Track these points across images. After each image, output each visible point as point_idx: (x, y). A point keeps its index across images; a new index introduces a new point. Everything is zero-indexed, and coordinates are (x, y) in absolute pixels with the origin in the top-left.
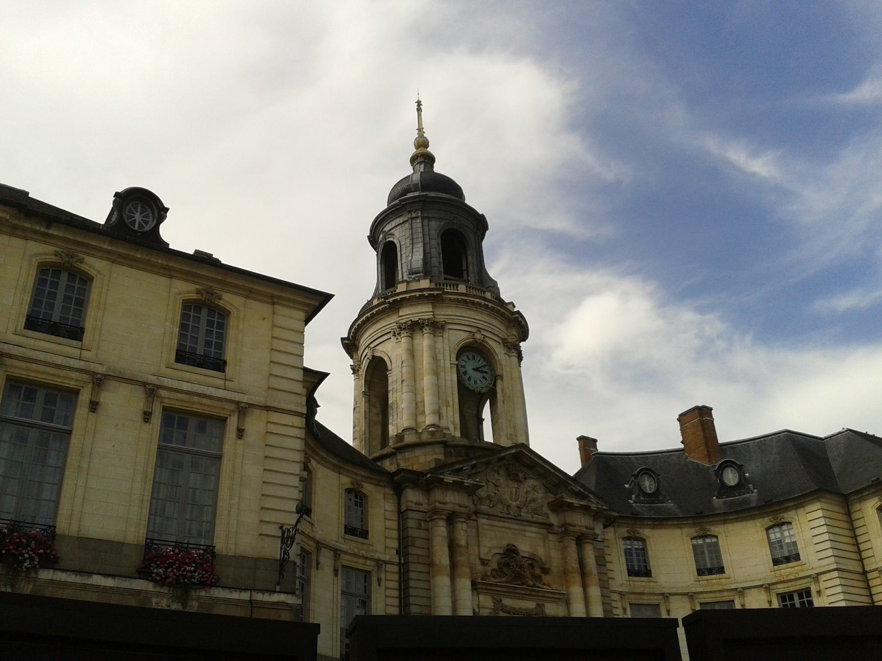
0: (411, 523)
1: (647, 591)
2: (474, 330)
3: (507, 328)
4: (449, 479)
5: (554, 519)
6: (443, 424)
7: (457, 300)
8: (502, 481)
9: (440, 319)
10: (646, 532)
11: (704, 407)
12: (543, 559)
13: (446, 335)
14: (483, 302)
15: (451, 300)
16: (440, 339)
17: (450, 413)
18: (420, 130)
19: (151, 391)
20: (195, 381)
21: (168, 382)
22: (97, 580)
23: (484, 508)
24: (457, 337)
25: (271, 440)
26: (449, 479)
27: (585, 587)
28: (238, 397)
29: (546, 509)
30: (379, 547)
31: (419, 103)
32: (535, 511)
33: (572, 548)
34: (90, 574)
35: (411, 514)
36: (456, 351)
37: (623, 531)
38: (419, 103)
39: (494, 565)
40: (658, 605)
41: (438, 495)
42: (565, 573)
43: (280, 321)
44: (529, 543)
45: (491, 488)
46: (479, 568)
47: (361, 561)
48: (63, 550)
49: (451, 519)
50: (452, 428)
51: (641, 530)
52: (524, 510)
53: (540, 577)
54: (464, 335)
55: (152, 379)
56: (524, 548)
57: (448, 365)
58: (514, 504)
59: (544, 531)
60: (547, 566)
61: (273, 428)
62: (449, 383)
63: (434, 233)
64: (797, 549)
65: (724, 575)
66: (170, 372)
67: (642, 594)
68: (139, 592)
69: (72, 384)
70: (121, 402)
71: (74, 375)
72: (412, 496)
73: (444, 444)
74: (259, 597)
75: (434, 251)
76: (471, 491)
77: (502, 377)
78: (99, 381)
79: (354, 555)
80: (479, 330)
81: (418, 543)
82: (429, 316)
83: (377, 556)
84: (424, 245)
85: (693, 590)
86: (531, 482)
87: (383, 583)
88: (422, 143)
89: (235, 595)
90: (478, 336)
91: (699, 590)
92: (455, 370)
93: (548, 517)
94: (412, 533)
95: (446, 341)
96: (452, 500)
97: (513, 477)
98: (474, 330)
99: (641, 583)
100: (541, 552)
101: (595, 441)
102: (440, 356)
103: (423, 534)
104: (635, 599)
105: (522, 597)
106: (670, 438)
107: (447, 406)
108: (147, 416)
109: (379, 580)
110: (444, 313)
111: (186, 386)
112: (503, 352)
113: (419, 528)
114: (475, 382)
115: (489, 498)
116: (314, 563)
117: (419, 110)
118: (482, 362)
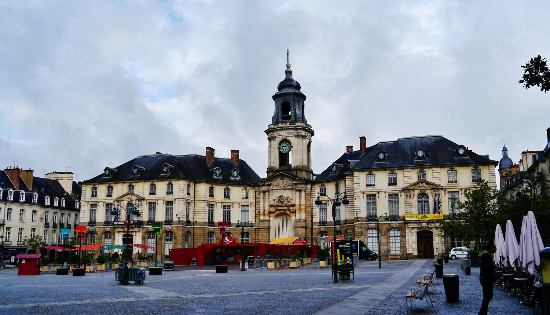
4: (261, 184)
10: (326, 184)
23: (274, 188)
26: (261, 184)
31: (288, 51)
33: (298, 193)
37: (320, 185)
38: (288, 51)
46: (273, 201)
49: (264, 192)
72: (257, 188)
73: (272, 171)
76: (270, 185)
88: (288, 66)
90: (284, 138)
96: (264, 188)
117: (288, 53)
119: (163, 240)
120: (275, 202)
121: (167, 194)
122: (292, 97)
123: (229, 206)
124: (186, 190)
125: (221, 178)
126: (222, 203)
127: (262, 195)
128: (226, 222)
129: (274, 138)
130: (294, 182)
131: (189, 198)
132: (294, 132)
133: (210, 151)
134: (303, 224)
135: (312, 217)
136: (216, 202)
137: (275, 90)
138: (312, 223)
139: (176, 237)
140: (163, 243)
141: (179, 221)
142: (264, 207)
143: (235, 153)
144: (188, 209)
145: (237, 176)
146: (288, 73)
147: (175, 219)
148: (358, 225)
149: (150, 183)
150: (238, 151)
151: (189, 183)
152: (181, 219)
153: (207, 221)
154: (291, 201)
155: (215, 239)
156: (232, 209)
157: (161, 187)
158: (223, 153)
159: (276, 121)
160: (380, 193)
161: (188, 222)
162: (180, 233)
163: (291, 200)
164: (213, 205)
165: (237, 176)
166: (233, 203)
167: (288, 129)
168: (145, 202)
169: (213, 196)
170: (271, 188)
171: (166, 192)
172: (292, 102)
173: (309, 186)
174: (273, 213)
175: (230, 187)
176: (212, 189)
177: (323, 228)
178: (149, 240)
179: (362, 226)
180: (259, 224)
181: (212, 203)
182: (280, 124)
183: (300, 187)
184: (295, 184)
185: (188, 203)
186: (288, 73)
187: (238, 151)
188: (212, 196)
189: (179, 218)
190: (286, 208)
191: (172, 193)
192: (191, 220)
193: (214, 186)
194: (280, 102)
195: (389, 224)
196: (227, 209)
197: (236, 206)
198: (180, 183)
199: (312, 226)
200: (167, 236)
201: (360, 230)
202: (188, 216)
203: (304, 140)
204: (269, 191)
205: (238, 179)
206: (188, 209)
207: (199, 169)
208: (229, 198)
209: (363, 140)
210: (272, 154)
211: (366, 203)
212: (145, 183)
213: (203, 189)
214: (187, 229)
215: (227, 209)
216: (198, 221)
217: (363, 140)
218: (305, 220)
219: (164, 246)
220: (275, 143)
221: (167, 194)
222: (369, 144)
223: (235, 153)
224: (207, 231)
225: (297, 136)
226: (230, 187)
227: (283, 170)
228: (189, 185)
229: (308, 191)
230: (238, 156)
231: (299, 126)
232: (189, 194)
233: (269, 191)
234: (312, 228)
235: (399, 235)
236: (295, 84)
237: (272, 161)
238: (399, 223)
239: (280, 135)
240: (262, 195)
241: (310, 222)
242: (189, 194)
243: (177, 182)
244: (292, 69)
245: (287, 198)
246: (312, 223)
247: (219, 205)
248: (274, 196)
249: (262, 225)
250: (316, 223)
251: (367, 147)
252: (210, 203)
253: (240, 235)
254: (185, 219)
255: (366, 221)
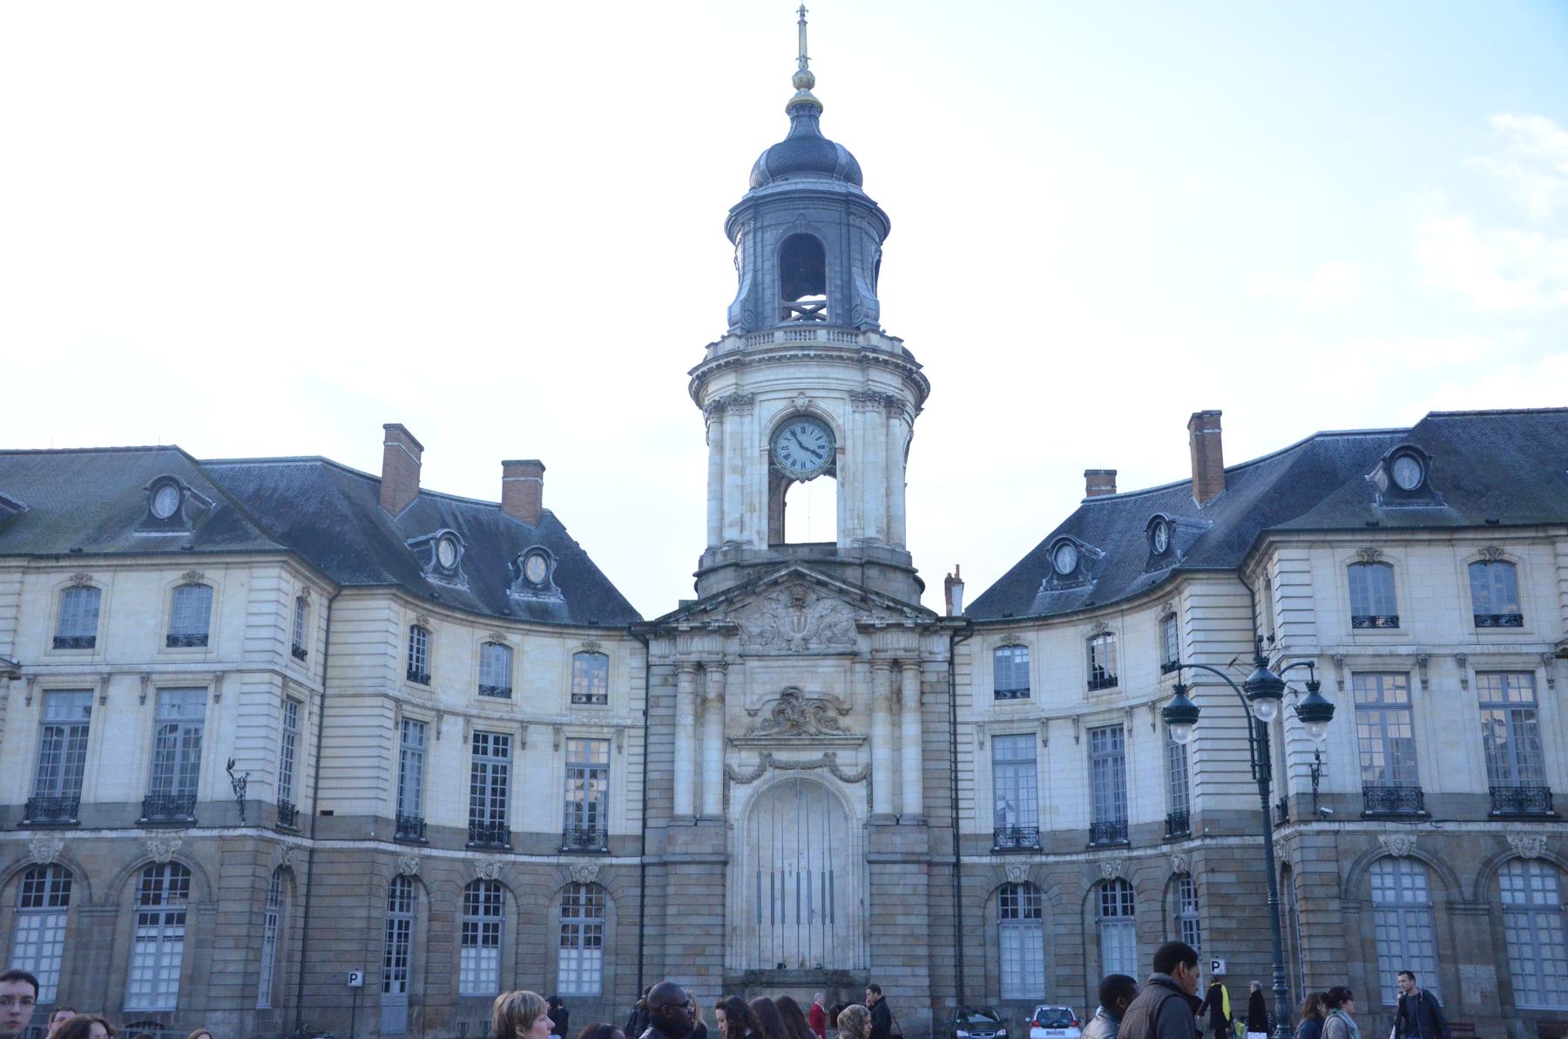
0: (653, 681)
1: (1016, 717)
2: (795, 394)
3: (863, 370)
5: (864, 644)
6: (746, 536)
7: (770, 359)
8: (781, 611)
9: (747, 390)
10: (1029, 636)
11: (1205, 413)
12: (842, 698)
13: (756, 410)
14: (800, 353)
15: (760, 361)
16: (747, 420)
17: (756, 520)
18: (804, 59)
19: (145, 678)
20: (186, 660)
21: (158, 668)
22: (106, 834)
23: (754, 648)
24: (771, 410)
25: (245, 699)
26: (684, 626)
27: (896, 724)
28: (214, 667)
29: (853, 633)
30: (623, 712)
31: (802, 11)
32: (830, 640)
33: (883, 678)
34: (99, 829)
35: (654, 670)
36: (768, 432)
37: (996, 638)
38: (802, 11)
39: (768, 715)
40: (1034, 734)
41: (680, 641)
42: (870, 711)
43: (256, 584)
44: (820, 679)
45: (768, 620)
46: (746, 720)
47: (595, 729)
48: (84, 816)
50: (755, 538)
51: (1022, 635)
52: (814, 640)
53: (834, 721)
54: (781, 405)
55: (145, 668)
56: (812, 687)
57: (756, 453)
58: (799, 636)
59: (847, 663)
60: (846, 706)
61: (246, 689)
62: (756, 479)
63: (768, 249)
64: (1028, 682)
65: (1115, 689)
66: (162, 657)
67: (1012, 721)
68: (135, 839)
69: (88, 686)
70: (123, 692)
71: (89, 678)
72: (658, 648)
74: (226, 833)
75: (768, 279)
76: (730, 631)
77: (843, 450)
78: (106, 679)
79: (583, 725)
80: (802, 392)
81: (664, 702)
82: (730, 392)
83: (615, 722)
84: (755, 271)
85: (1079, 711)
86: (828, 603)
87: (625, 751)
88: (805, 81)
89: (207, 833)
90: (801, 402)
91: (1085, 711)
92: (766, 458)
93: (855, 643)
94: (654, 691)
95: (756, 419)
96: (700, 647)
97: (799, 603)
98: (795, 394)
99: (1010, 706)
100: (839, 690)
101: (1112, 474)
102: (747, 444)
103: (669, 690)
104: (998, 729)
105: (804, 747)
106: (1177, 466)
107: (752, 511)
108: (143, 699)
109: (620, 748)
110: (754, 380)
111: (171, 668)
112: (849, 409)
113: (665, 683)
114: (803, 465)
115: (761, 635)
116: (518, 743)
117: (803, 23)
118: (817, 434)
119: (126, 921)
120: (758, 720)
121: (173, 641)
122: (833, 213)
123: (502, 743)
124: (288, 624)
125: (462, 586)
126: (468, 718)
127: (685, 684)
128: (489, 831)
129: (742, 402)
130: (865, 619)
131: (295, 671)
132: (850, 377)
133: (402, 446)
134: (916, 842)
135: (955, 806)
136: (440, 714)
137: (739, 188)
138: (957, 837)
139: (211, 901)
140: (121, 940)
141: (241, 803)
142: (699, 750)
143: (524, 475)
144: (290, 739)
145: (546, 587)
146: (805, 110)
147: (213, 786)
148: (1321, 841)
149: (59, 579)
150: (538, 467)
151: (306, 590)
152: (251, 794)
153: (390, 811)
154: (844, 722)
155: (423, 915)
156: (517, 754)
157: (135, 604)
158: (462, 472)
159: (749, 318)
160: (1432, 662)
161: (286, 814)
162: (239, 876)
163: (844, 713)
164: (422, 725)
165: (546, 587)
166: (524, 725)
167: (829, 357)
168: (18, 690)
169: (426, 680)
170: (734, 646)
171: (165, 631)
172: (829, 238)
173: (939, 646)
174: (749, 781)
175: (513, 638)
176: (419, 632)
177: (1017, 868)
178: (24, 922)
179: (1344, 843)
180: (671, 840)
181: (418, 714)
182: (779, 335)
183: (898, 643)
184: (864, 629)
185: (292, 705)
186: (805, 110)
187: (538, 467)
188: (417, 675)
189: (240, 785)
190: (817, 755)
191: (204, 640)
192: (303, 805)
193: (433, 623)
194: (771, 237)
195: (1498, 838)
196: (493, 750)
197: (540, 738)
198: (256, 584)
199: (957, 854)
200: (150, 895)
201: (1331, 867)
202: (287, 779)
203: (895, 422)
204: (724, 666)
205: (554, 599)
206: (290, 739)
207: (343, 529)
208: (507, 693)
209: (1205, 427)
210: (730, 480)
211: (1084, 764)
212: (31, 578)
213: (378, 623)
214: (275, 858)
215: (493, 750)
216: (340, 809)
217: (1205, 427)
218: (923, 822)
219: (129, 956)
220: (752, 429)
221: (173, 641)
222: (1240, 447)
223: (524, 475)
224: (389, 873)
225: (863, 398)
226: (513, 638)
227: (747, 577)
228: (302, 602)
229: (939, 668)
230: (537, 489)
231: (875, 350)
232: (299, 653)
233: (724, 666)
234: (957, 865)
235: (1553, 899)
236: (843, 160)
237: (732, 515)
238: (1553, 836)
239: (777, 388)
240: (685, 684)
241: (949, 834)
242: (299, 653)
243: (240, 575)
244: (817, 93)
245: (821, 705)
246: (957, 837)
247: (453, 729)
248: (754, 687)
249: (683, 844)
250: (977, 837)
251: (1229, 461)
252: (408, 711)
253: (559, 898)
254: (270, 795)
255: (1364, 817)
